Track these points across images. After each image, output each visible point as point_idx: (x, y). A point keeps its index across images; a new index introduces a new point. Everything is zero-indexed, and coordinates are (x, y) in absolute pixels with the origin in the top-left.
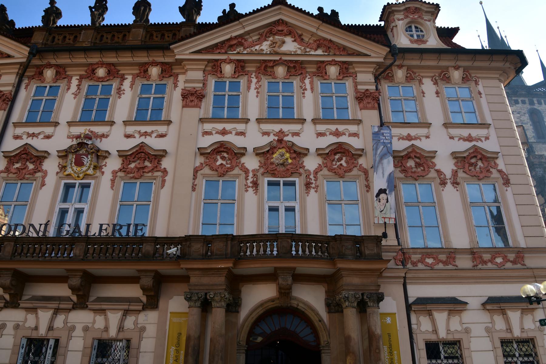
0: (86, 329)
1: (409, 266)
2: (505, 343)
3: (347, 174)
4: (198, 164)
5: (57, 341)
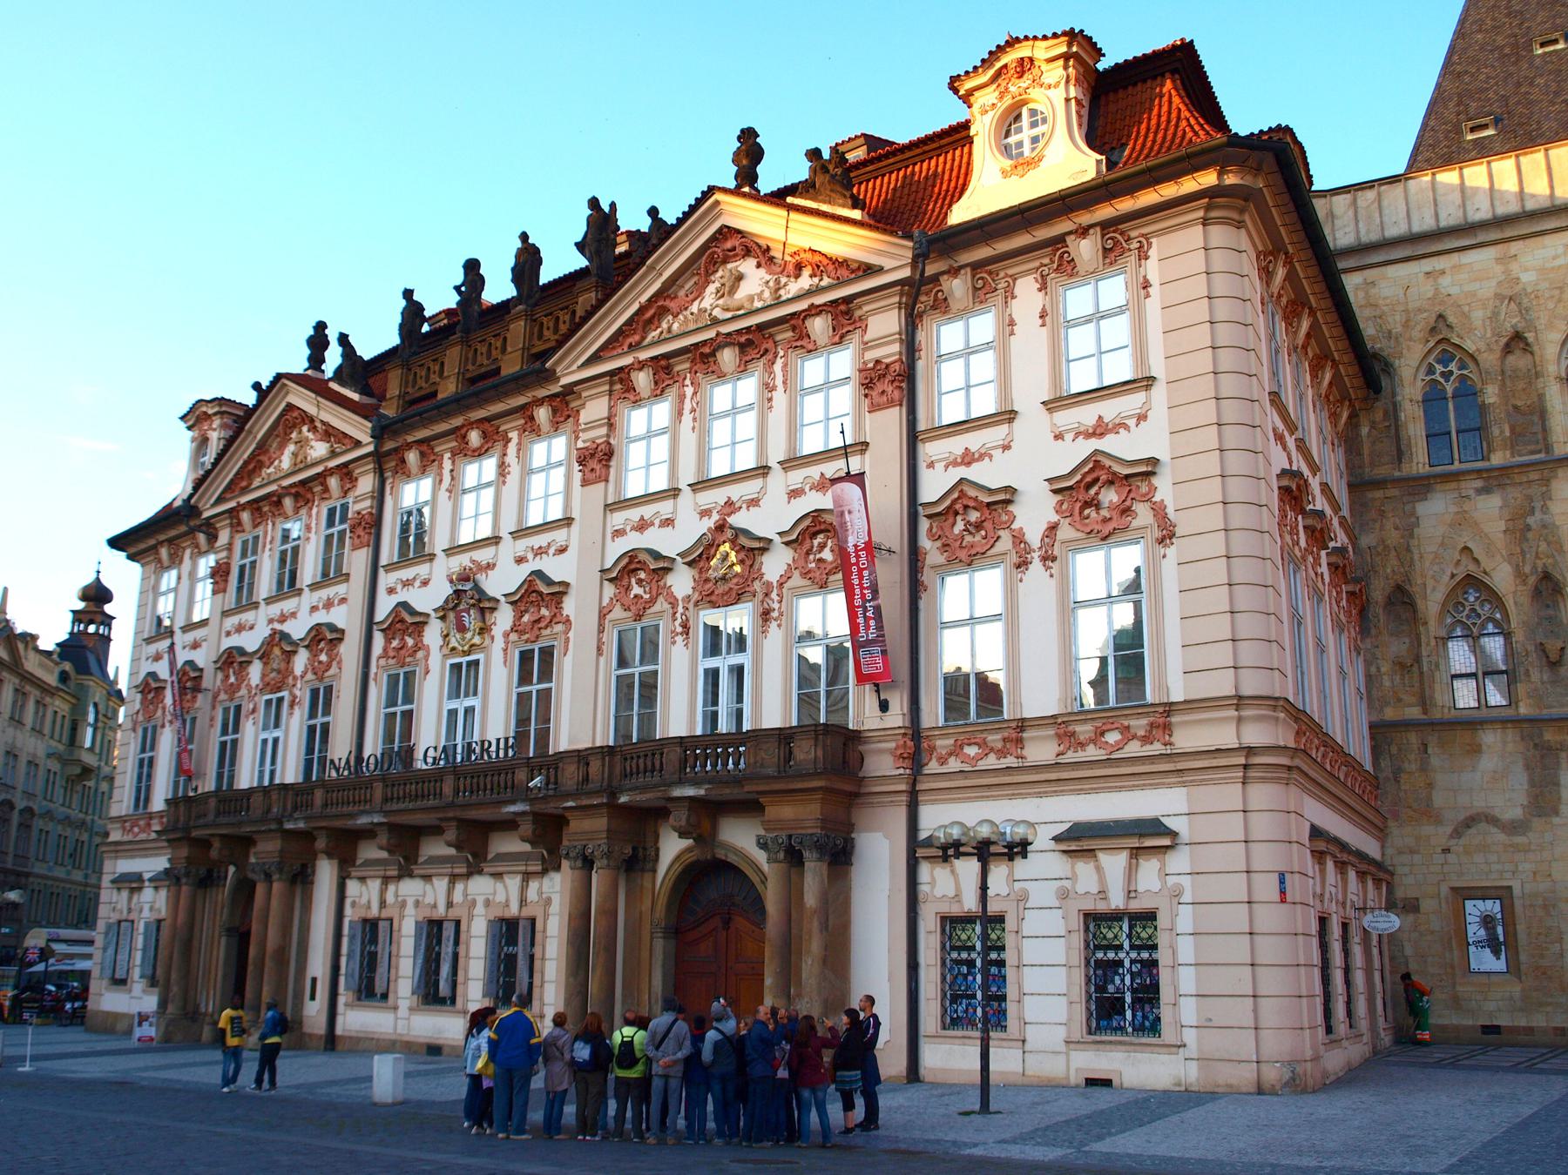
0: (487, 903)
1: (933, 767)
2: (1095, 920)
3: (832, 578)
4: (606, 601)
5: (458, 923)
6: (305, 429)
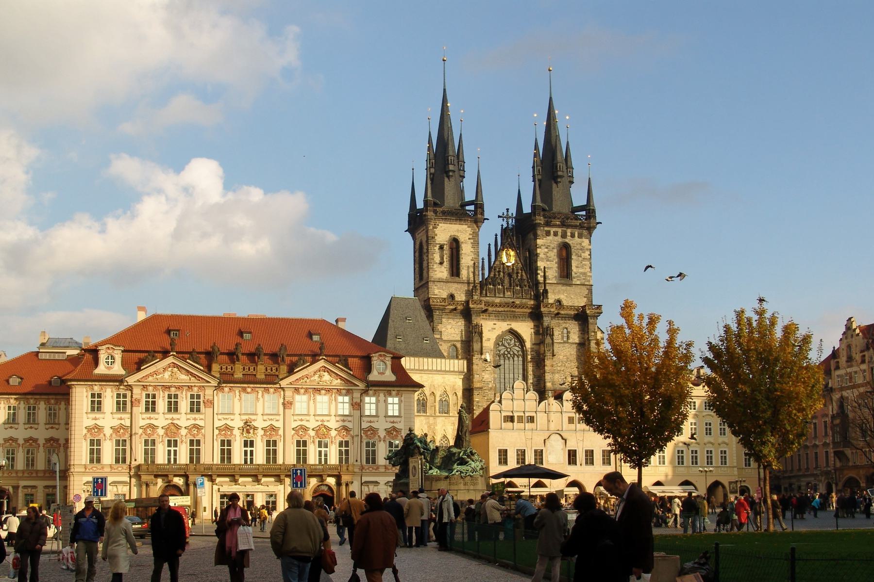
6: (176, 369)
